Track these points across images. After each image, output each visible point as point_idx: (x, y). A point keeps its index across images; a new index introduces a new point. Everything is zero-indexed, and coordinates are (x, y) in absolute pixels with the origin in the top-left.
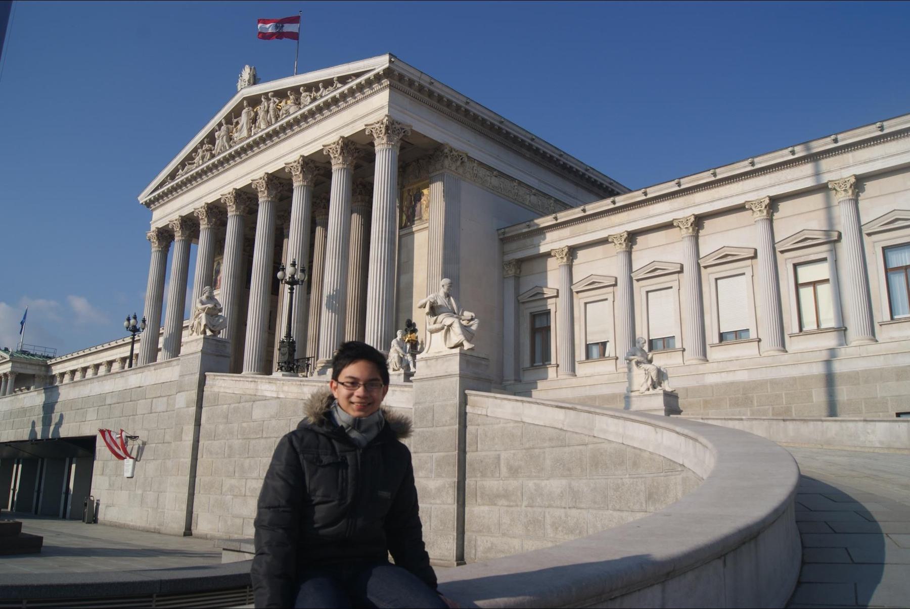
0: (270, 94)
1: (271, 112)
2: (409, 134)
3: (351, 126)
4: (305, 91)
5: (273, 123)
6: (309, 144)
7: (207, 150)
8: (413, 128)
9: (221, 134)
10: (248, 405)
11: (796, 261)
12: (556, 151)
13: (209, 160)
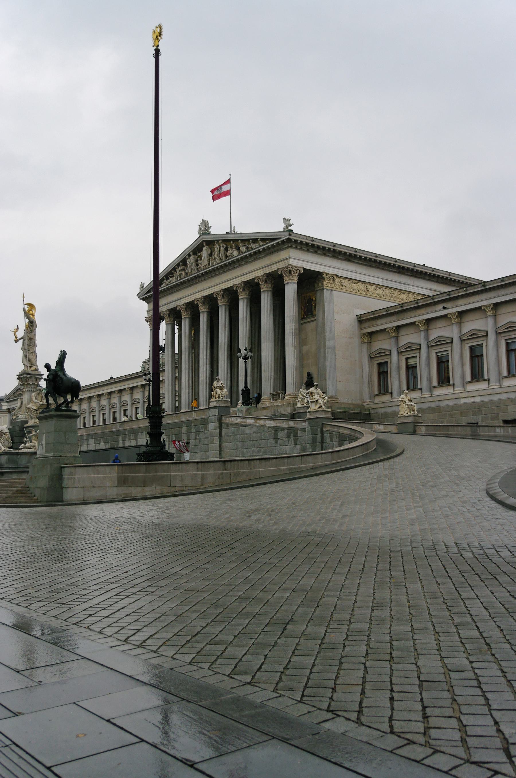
0: (220, 241)
3: (270, 267)
4: (241, 242)
5: (224, 260)
6: (246, 274)
7: (182, 270)
9: (191, 260)
11: (506, 338)
13: (184, 277)
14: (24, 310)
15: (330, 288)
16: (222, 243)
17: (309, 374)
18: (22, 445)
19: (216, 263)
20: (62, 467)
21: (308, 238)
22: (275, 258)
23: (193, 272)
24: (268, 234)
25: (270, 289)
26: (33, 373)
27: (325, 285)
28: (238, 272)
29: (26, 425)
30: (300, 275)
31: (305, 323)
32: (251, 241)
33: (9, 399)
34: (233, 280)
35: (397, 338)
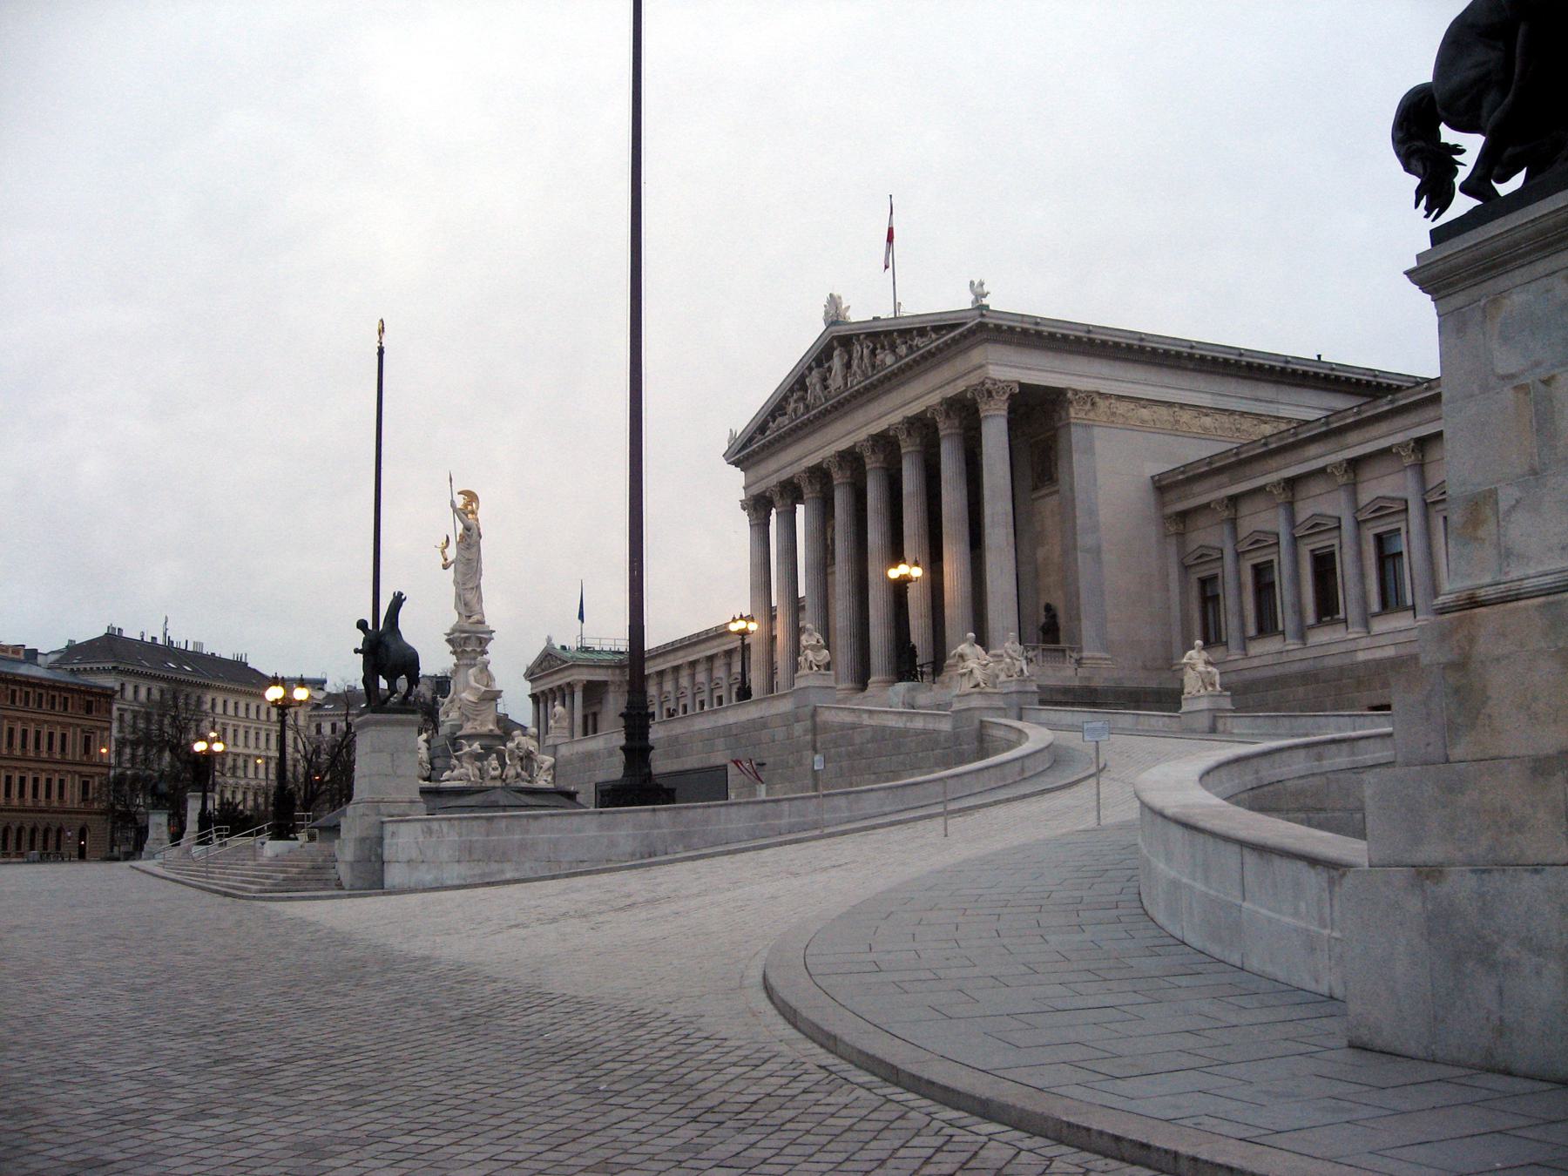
0: (862, 337)
1: (866, 360)
2: (1018, 390)
3: (952, 385)
5: (870, 374)
8: (1022, 381)
9: (814, 379)
10: (850, 732)
12: (1233, 351)
13: (803, 415)
14: (453, 504)
15: (1086, 422)
16: (865, 338)
17: (1048, 608)
18: (447, 774)
19: (857, 382)
20: (383, 823)
21: (1025, 319)
22: (960, 364)
23: (818, 403)
24: (944, 316)
25: (958, 431)
26: (474, 628)
27: (1073, 415)
28: (895, 398)
29: (459, 734)
30: (1012, 396)
31: (1043, 497)
32: (915, 332)
33: (532, 674)
34: (889, 416)
35: (1233, 522)
